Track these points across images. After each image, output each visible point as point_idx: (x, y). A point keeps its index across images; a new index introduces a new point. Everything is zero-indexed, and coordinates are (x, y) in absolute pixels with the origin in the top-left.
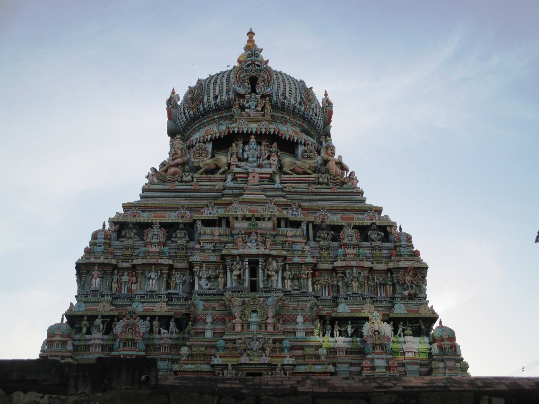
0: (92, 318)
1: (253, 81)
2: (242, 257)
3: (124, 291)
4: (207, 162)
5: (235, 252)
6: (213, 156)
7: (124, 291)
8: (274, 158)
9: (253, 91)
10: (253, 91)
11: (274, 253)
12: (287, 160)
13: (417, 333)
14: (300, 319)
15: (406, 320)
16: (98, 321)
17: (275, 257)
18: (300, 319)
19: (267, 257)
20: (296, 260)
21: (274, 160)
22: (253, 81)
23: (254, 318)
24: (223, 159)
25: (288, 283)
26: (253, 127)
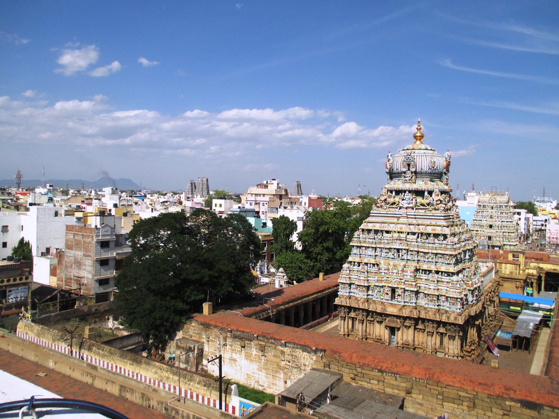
0: (355, 262)
1: (409, 165)
2: (395, 249)
3: (364, 253)
4: (391, 200)
5: (392, 247)
6: (394, 197)
7: (364, 253)
8: (414, 200)
9: (409, 170)
10: (409, 170)
11: (404, 248)
12: (419, 199)
13: (449, 275)
14: (409, 272)
15: (445, 272)
16: (356, 263)
17: (405, 249)
18: (409, 272)
19: (402, 249)
20: (412, 249)
21: (414, 201)
22: (409, 165)
23: (395, 271)
24: (397, 199)
25: (409, 256)
26: (407, 186)
